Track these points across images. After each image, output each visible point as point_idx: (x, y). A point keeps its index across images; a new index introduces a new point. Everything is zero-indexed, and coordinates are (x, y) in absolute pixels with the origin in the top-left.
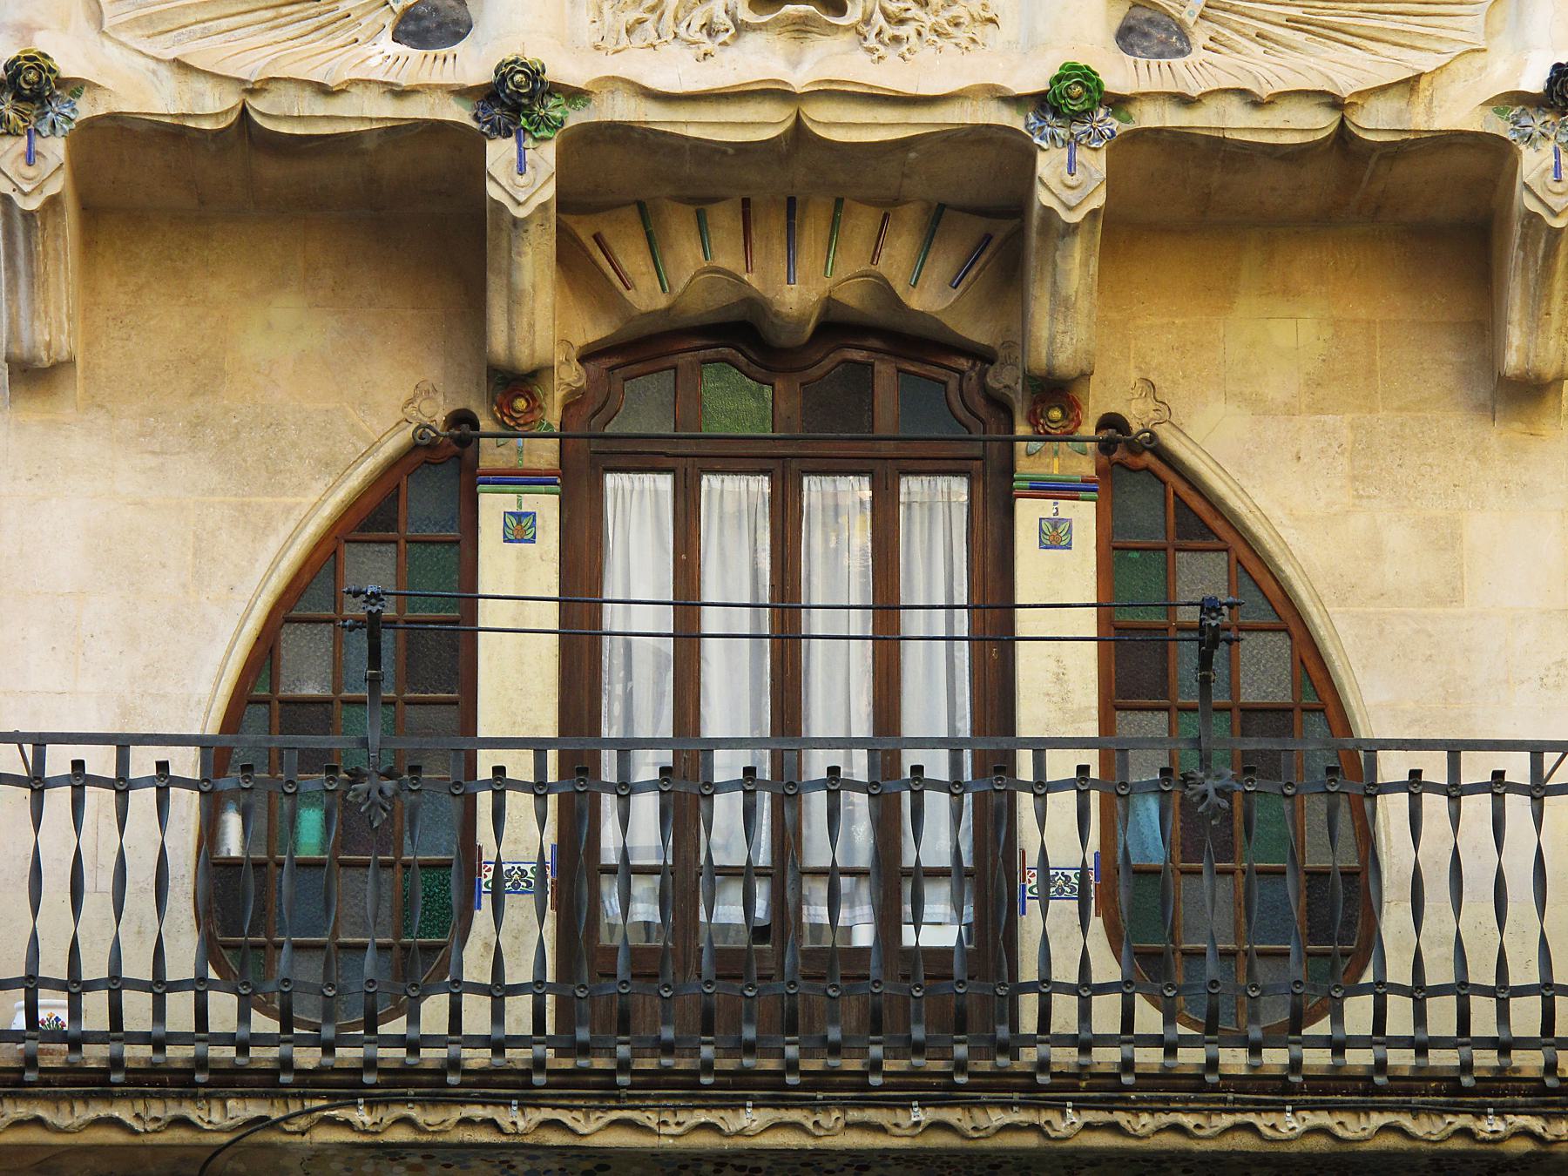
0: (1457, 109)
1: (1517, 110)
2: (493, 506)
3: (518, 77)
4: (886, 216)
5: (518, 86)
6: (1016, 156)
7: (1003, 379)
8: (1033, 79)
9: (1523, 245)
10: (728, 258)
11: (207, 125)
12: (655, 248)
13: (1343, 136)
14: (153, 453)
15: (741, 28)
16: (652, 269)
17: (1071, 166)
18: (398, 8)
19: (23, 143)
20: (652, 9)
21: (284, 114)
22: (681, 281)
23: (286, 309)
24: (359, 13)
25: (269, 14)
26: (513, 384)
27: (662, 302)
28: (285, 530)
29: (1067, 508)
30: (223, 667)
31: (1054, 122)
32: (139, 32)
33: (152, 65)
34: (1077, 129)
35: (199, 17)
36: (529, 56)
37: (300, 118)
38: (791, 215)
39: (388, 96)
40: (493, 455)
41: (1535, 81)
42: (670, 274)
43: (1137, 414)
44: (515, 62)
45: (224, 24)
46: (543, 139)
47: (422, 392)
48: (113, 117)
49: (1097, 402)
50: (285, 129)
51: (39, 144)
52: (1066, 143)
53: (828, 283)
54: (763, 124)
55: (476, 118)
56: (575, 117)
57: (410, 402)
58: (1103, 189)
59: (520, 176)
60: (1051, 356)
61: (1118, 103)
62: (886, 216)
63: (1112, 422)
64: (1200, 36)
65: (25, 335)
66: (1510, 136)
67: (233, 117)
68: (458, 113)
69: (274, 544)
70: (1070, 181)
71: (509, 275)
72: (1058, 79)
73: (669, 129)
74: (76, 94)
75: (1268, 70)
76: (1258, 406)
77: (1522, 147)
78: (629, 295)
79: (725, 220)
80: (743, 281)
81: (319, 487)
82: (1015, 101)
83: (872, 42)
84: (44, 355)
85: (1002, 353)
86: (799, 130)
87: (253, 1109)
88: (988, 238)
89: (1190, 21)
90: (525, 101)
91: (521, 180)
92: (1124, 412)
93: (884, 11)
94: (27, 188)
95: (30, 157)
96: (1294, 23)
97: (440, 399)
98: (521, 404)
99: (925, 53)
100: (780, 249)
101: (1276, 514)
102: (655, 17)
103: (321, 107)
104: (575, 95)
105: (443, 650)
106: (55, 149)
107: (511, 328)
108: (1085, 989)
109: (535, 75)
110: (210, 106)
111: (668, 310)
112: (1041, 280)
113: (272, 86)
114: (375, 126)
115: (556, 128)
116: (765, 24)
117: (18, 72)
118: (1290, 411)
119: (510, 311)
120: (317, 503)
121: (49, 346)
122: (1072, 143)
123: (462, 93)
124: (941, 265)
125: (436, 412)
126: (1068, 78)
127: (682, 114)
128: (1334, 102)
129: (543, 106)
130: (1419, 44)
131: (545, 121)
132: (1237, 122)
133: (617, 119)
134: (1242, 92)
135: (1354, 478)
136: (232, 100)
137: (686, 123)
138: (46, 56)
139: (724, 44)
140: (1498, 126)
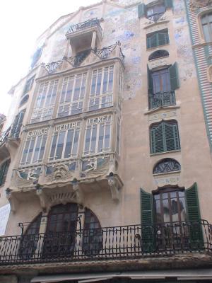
0: (104, 178)
2: (42, 219)
6: (71, 186)
8: (72, 179)
21: (25, 190)
40: (43, 215)
41: (108, 174)
43: (88, 207)
54: (54, 186)
61: (79, 181)
63: (86, 208)
75: (90, 177)
82: (72, 182)
105: (38, 229)
108: (79, 251)
110: (20, 190)
128: (95, 178)
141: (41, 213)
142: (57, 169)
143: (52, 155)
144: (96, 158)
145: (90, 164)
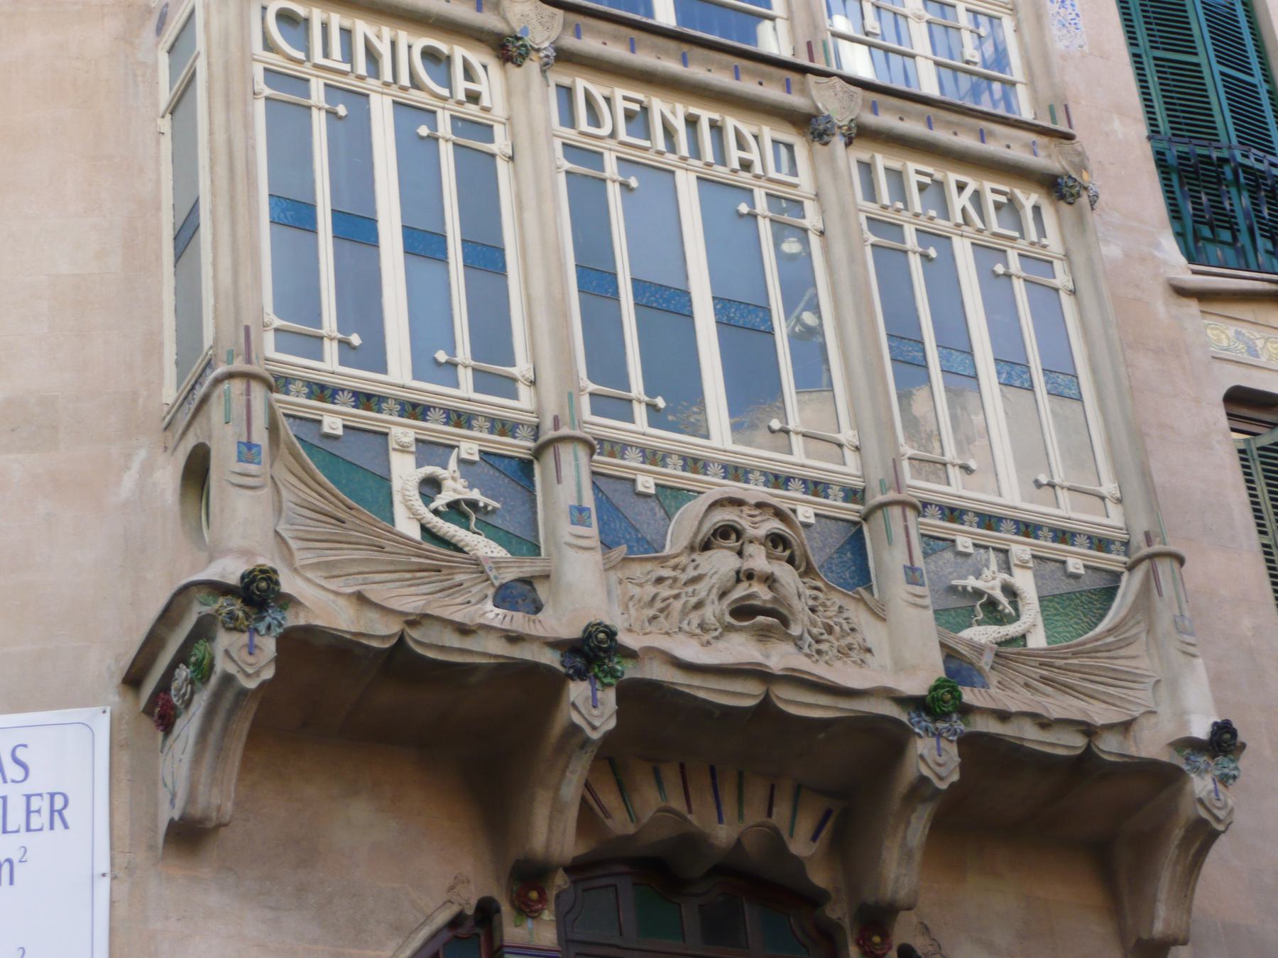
0: (1151, 744)
1: (1188, 751)
3: (602, 636)
4: (773, 787)
5: (601, 642)
7: (838, 912)
9: (1180, 846)
10: (677, 804)
11: (375, 644)
12: (623, 791)
13: (1088, 755)
14: (270, 907)
15: (729, 628)
16: (622, 805)
17: (939, 749)
18: (497, 583)
19: (245, 638)
20: (662, 610)
21: (433, 644)
22: (647, 815)
23: (360, 810)
24: (469, 584)
25: (408, 575)
26: (528, 880)
27: (631, 829)
31: (927, 718)
32: (320, 574)
33: (331, 597)
34: (940, 725)
35: (361, 569)
36: (608, 622)
37: (442, 648)
38: (713, 777)
39: (503, 640)
41: (1201, 729)
42: (645, 811)
44: (599, 624)
45: (379, 577)
46: (610, 685)
47: (459, 881)
48: (309, 630)
50: (431, 654)
51: (257, 639)
52: (934, 735)
54: (745, 695)
55: (562, 663)
56: (630, 671)
57: (452, 888)
59: (591, 708)
62: (773, 787)
64: (993, 678)
65: (202, 800)
66: (1185, 767)
67: (394, 641)
68: (550, 658)
70: (940, 760)
71: (557, 789)
72: (935, 688)
73: (687, 690)
74: (283, 608)
77: (1193, 775)
78: (609, 822)
79: (671, 775)
80: (686, 820)
81: (392, 945)
82: (904, 701)
83: (806, 650)
84: (214, 815)
85: (833, 895)
86: (766, 703)
88: (828, 814)
89: (987, 668)
90: (602, 654)
91: (595, 712)
92: (912, 944)
93: (810, 633)
94: (250, 671)
95: (251, 649)
96: (1045, 680)
97: (472, 888)
99: (838, 664)
100: (710, 799)
102: (662, 616)
103: (453, 640)
104: (630, 654)
106: (269, 646)
107: (550, 830)
109: (611, 634)
110: (380, 630)
111: (637, 833)
113: (425, 622)
114: (492, 661)
115: (617, 678)
116: (745, 627)
117: (253, 580)
119: (551, 818)
121: (219, 808)
122: (938, 735)
123: (556, 644)
124: (805, 826)
125: (469, 898)
126: (943, 687)
127: (696, 681)
128: (1089, 730)
129: (610, 660)
130: (1118, 703)
131: (612, 673)
132: (1030, 734)
133: (654, 677)
134: (1034, 716)
136: (392, 627)
137: (699, 688)
138: (275, 572)
139: (716, 638)
140: (1179, 761)
141: (486, 912)
142: (725, 532)
143: (604, 360)
144: (1021, 550)
145: (991, 582)
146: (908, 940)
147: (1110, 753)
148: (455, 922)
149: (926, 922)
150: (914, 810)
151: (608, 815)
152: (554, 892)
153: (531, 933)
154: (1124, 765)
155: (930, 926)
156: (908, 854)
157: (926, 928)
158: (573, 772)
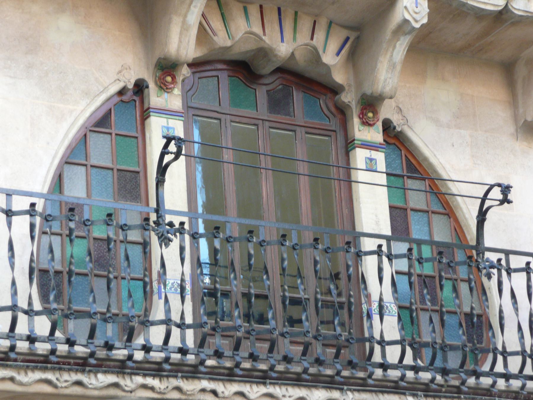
4: (315, 22)
7: (349, 98)
14: (11, 77)
16: (224, 28)
22: (238, 35)
26: (167, 69)
27: (229, 43)
28: (70, 120)
29: (375, 154)
30: (46, 178)
43: (396, 119)
47: (124, 68)
49: (387, 111)
53: (295, 45)
57: (120, 72)
58: (427, 17)
60: (384, 87)
62: (315, 22)
69: (65, 126)
70: (417, 10)
71: (185, 16)
76: (437, 122)
78: (215, 38)
80: (261, 39)
81: (83, 103)
85: (347, 88)
87: (111, 378)
88: (347, 39)
92: (391, 119)
97: (132, 72)
98: (169, 79)
100: (277, 28)
101: (448, 167)
107: (180, 41)
112: (386, 54)
118: (449, 127)
119: (181, 34)
120: (82, 110)
124: (333, 45)
135: (473, 156)
141: (140, 87)
146: (388, 116)
147: (519, 10)
148: (121, 92)
149: (400, 106)
150: (398, 40)
151: (215, 34)
152: (181, 78)
153: (167, 101)
154: (527, 17)
155: (402, 109)
156: (393, 66)
157: (401, 110)
158: (195, 7)
